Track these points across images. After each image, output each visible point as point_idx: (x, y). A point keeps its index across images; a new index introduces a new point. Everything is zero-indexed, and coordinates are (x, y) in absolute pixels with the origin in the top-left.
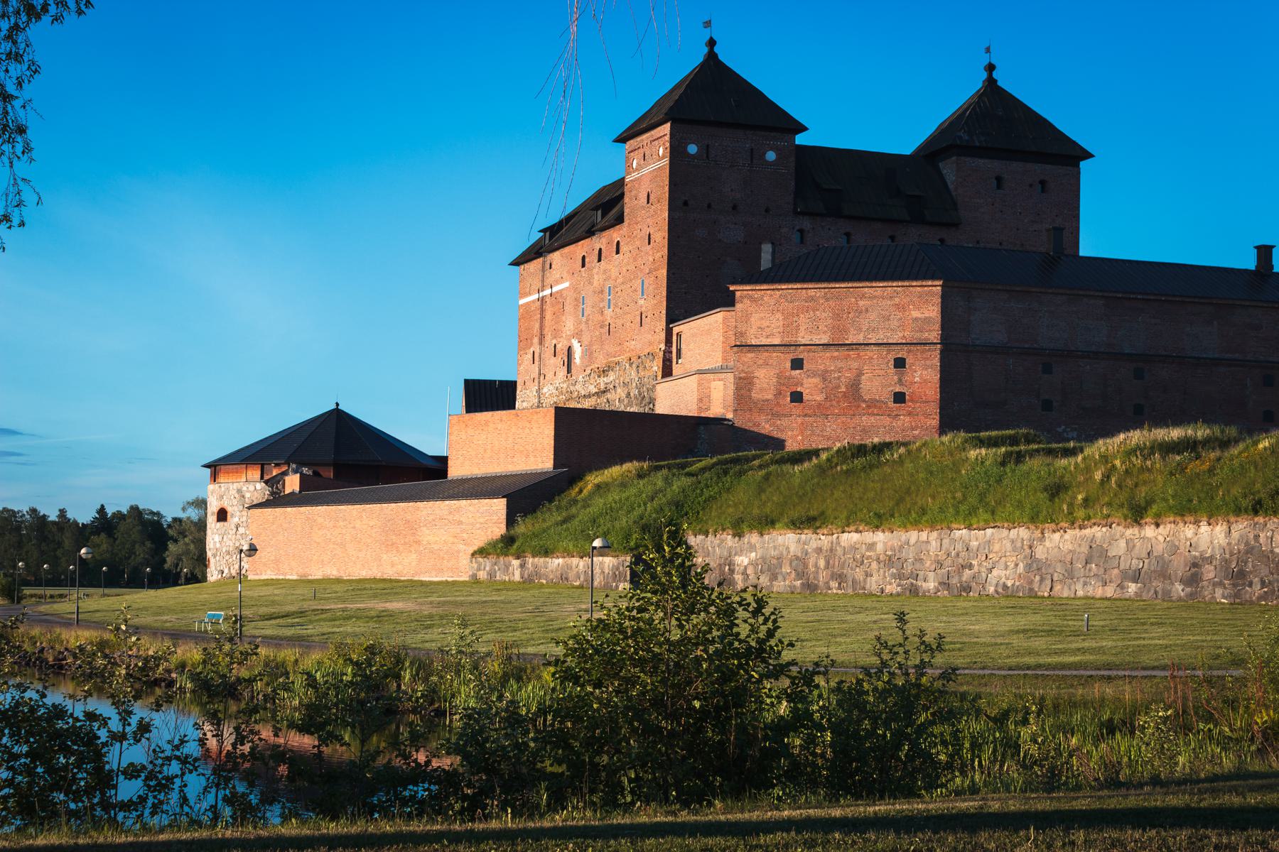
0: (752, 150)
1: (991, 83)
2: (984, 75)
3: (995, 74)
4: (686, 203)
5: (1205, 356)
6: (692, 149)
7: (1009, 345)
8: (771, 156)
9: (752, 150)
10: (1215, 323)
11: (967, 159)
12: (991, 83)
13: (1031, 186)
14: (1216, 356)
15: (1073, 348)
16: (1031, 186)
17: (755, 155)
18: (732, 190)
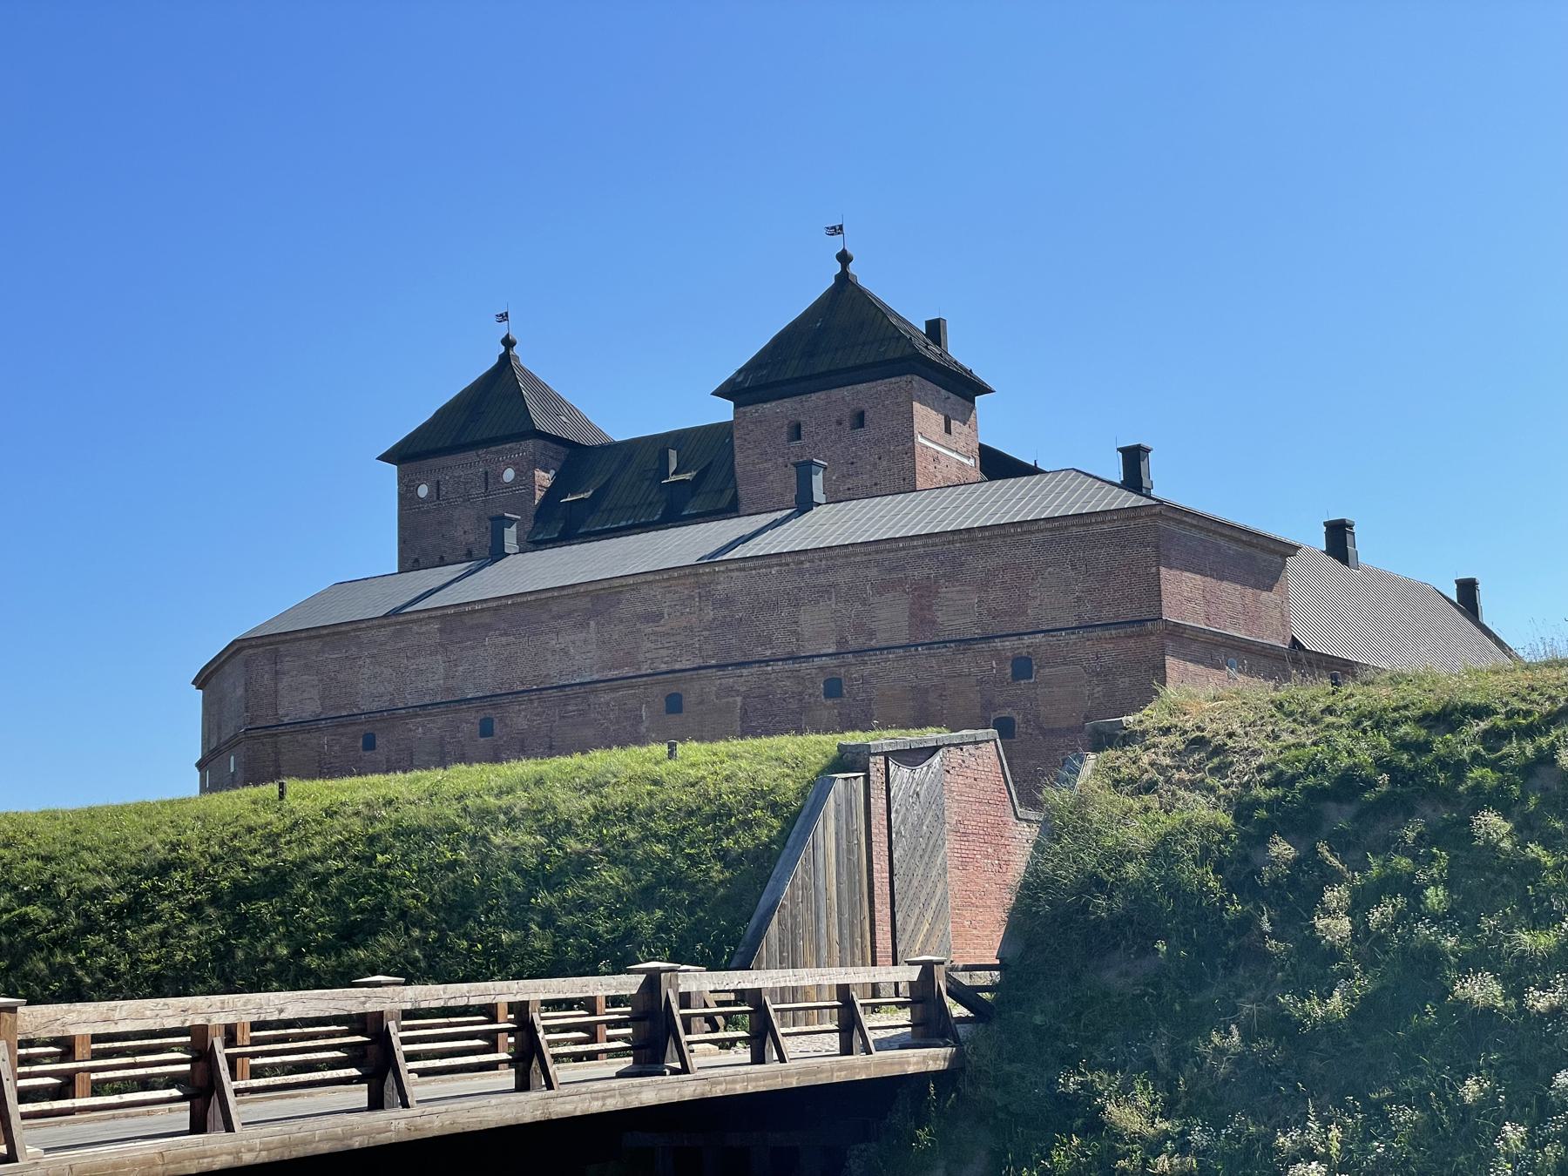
0: (486, 473)
1: (844, 279)
2: (838, 269)
3: (852, 268)
4: (417, 560)
5: (578, 681)
6: (423, 491)
7: (323, 716)
8: (509, 475)
9: (486, 473)
10: (592, 623)
11: (750, 408)
12: (844, 279)
13: (839, 423)
14: (596, 677)
15: (401, 705)
16: (839, 423)
17: (490, 479)
18: (465, 532)
